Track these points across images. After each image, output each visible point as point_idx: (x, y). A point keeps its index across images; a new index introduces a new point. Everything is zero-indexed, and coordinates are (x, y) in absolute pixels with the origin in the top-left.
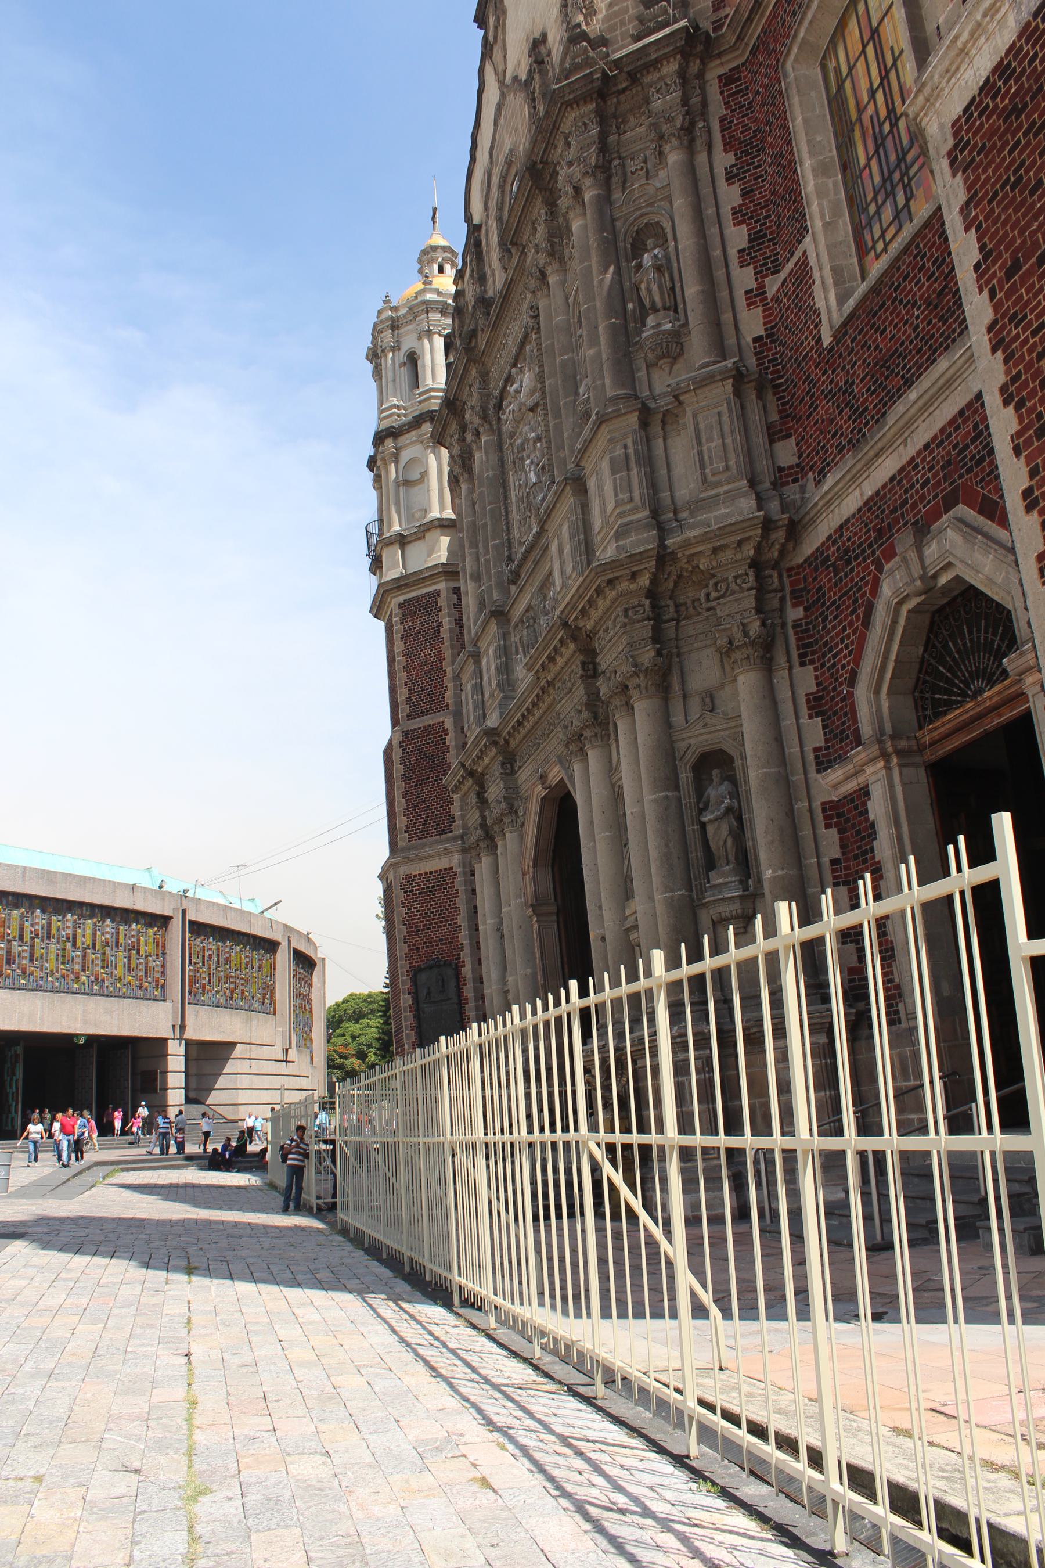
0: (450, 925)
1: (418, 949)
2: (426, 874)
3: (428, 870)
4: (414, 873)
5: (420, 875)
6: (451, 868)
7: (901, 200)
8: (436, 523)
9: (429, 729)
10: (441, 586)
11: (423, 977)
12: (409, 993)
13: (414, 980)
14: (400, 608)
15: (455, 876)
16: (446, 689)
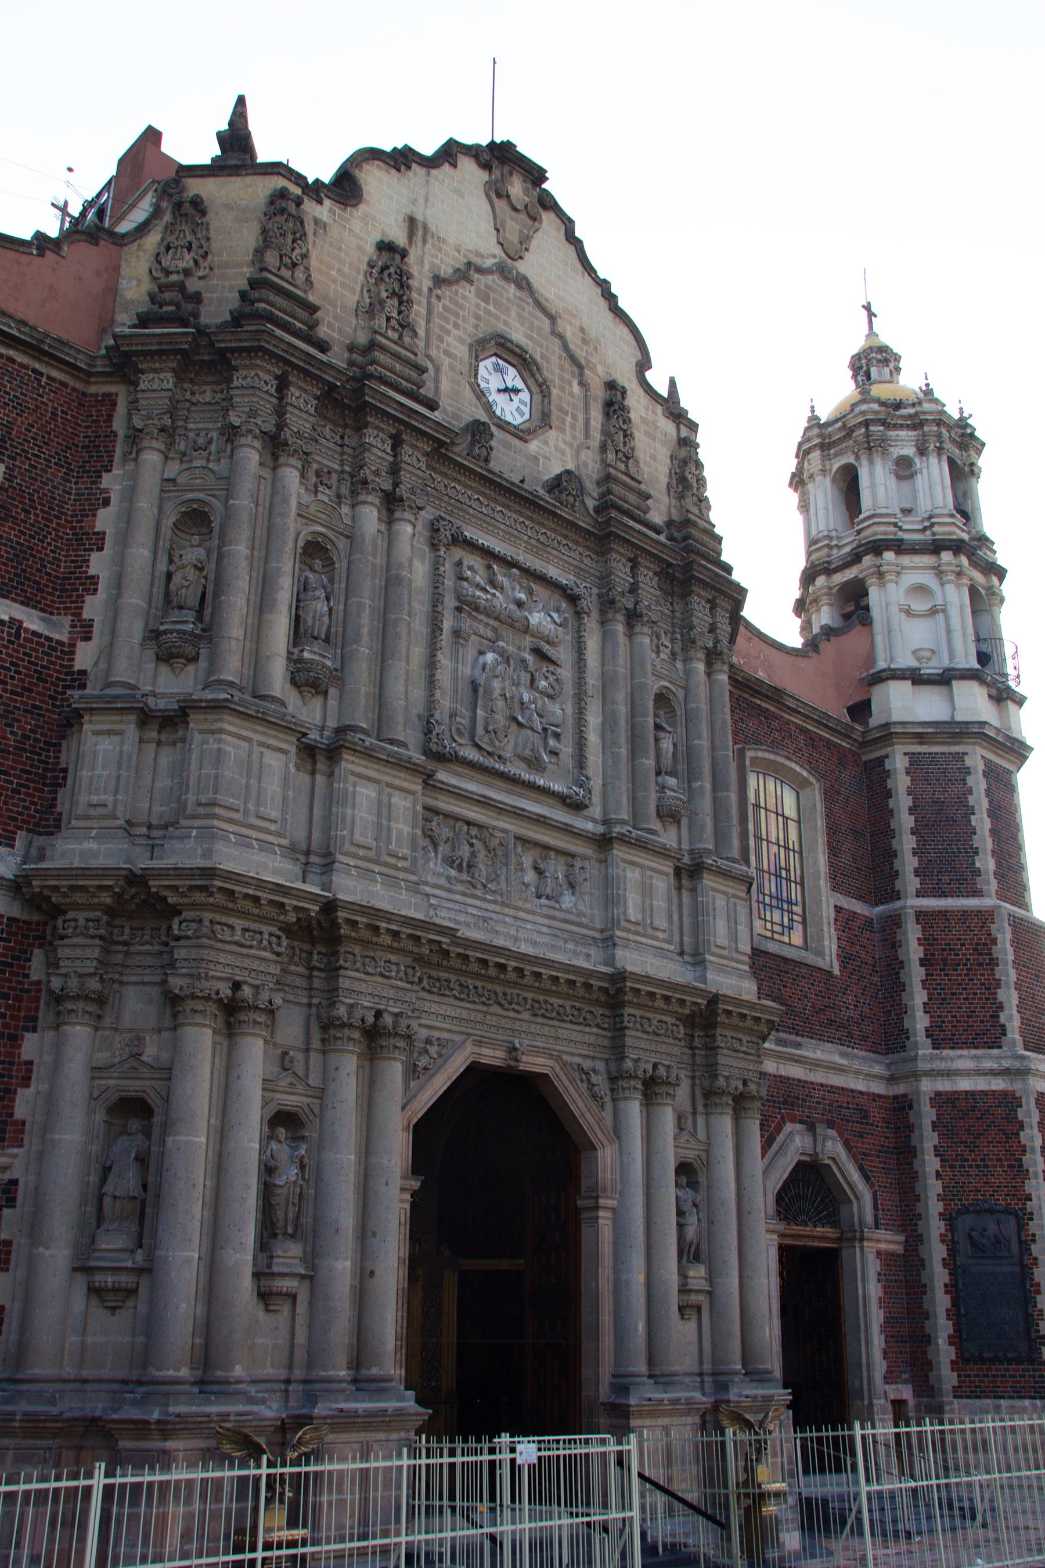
7: (786, 920)
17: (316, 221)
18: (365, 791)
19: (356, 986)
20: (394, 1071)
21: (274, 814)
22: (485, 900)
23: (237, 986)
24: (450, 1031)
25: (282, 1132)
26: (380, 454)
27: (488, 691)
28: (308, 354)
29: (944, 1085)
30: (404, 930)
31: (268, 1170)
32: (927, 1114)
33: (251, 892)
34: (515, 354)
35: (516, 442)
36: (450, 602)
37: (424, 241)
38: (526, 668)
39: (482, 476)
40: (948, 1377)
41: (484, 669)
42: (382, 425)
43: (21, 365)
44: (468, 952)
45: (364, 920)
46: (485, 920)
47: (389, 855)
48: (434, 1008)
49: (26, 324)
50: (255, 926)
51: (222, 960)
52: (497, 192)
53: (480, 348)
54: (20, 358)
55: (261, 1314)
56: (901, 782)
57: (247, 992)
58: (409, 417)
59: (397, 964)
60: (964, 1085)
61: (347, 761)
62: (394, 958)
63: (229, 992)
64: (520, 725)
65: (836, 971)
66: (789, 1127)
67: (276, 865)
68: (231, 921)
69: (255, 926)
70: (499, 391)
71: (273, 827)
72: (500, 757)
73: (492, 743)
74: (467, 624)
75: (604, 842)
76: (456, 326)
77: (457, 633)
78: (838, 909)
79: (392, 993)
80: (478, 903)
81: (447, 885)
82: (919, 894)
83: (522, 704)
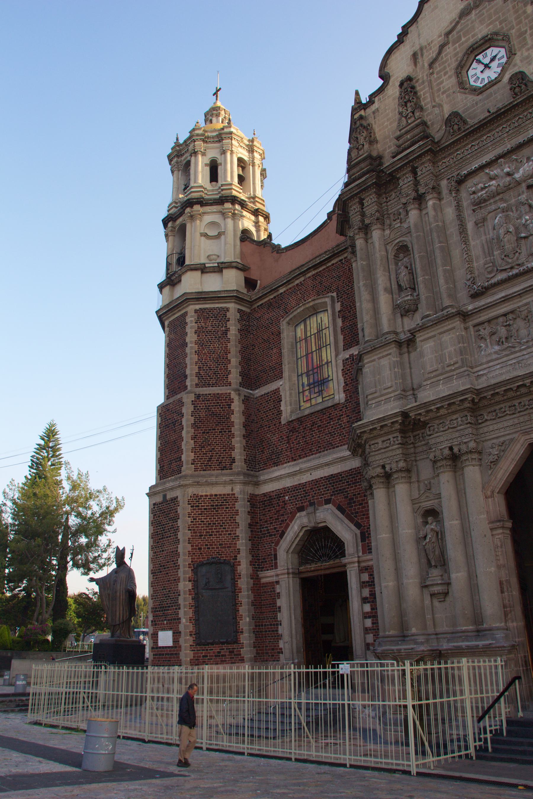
0: (230, 534)
1: (200, 549)
2: (211, 495)
3: (213, 493)
4: (200, 494)
5: (206, 496)
6: (234, 494)
8: (234, 264)
9: (217, 396)
10: (232, 306)
11: (204, 570)
12: (190, 581)
13: (195, 571)
14: (195, 312)
15: (236, 500)
16: (230, 372)
17: (374, 113)
18: (428, 345)
19: (438, 440)
21: (389, 384)
22: (521, 351)
23: (383, 467)
24: (509, 434)
25: (430, 519)
26: (406, 186)
27: (498, 238)
28: (357, 185)
30: (444, 403)
31: (420, 539)
33: (371, 427)
34: (483, 44)
35: (495, 87)
37: (422, 55)
38: (523, 204)
39: (465, 136)
41: (494, 229)
42: (404, 172)
43: (336, 263)
44: (496, 391)
45: (423, 411)
46: (519, 362)
47: (448, 366)
48: (496, 427)
49: (326, 252)
50: (385, 438)
51: (377, 459)
54: (334, 262)
55: (436, 603)
57: (388, 468)
58: (407, 159)
59: (457, 419)
61: (418, 337)
62: (455, 417)
63: (382, 471)
64: (525, 238)
67: (392, 406)
68: (376, 441)
69: (385, 438)
70: (482, 72)
71: (390, 390)
72: (519, 265)
73: (508, 263)
76: (445, 74)
77: (476, 224)
79: (457, 434)
80: (518, 354)
81: (497, 356)
83: (524, 225)
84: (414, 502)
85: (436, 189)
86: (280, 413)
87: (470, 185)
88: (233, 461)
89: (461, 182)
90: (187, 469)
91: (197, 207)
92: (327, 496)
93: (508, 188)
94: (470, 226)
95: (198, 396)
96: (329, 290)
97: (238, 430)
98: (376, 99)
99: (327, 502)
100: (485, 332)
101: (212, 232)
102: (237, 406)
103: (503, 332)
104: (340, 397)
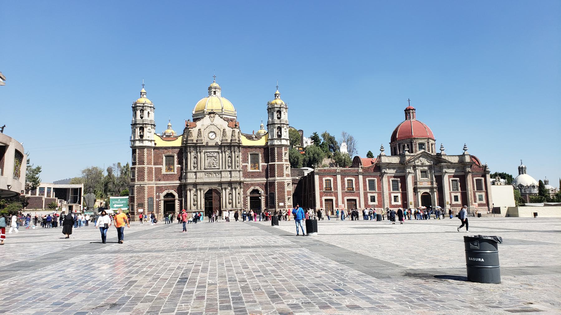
20: (202, 191)
29: (269, 181)
32: (268, 184)
36: (206, 157)
40: (269, 207)
52: (210, 117)
53: (209, 133)
56: (270, 151)
60: (271, 181)
64: (213, 164)
65: (261, 171)
66: (252, 187)
74: (208, 158)
75: (221, 171)
78: (262, 165)
82: (270, 162)
84: (193, 193)
85: (202, 152)
86: (161, 172)
87: (207, 153)
88: (153, 180)
89: (207, 152)
90: (146, 181)
91: (147, 125)
92: (172, 188)
93: (212, 156)
94: (206, 159)
95: (148, 167)
96: (175, 153)
97: (154, 174)
98: (194, 128)
99: (172, 189)
100: (206, 174)
101: (149, 131)
102: (154, 170)
103: (208, 175)
104: (176, 173)
